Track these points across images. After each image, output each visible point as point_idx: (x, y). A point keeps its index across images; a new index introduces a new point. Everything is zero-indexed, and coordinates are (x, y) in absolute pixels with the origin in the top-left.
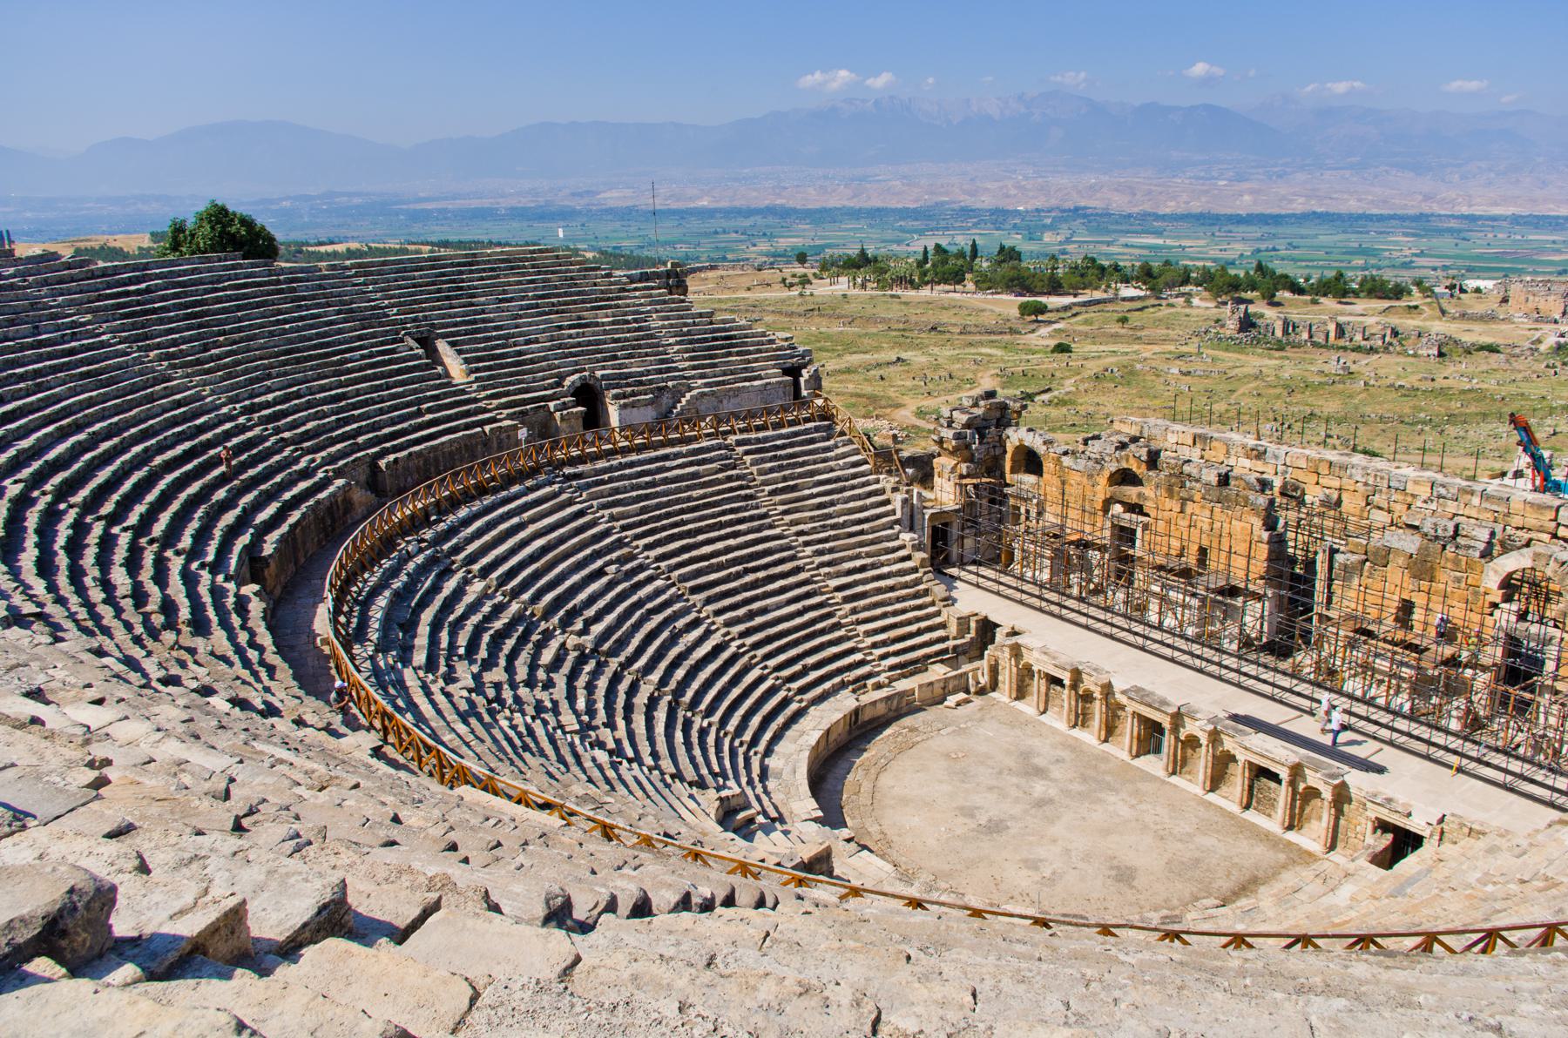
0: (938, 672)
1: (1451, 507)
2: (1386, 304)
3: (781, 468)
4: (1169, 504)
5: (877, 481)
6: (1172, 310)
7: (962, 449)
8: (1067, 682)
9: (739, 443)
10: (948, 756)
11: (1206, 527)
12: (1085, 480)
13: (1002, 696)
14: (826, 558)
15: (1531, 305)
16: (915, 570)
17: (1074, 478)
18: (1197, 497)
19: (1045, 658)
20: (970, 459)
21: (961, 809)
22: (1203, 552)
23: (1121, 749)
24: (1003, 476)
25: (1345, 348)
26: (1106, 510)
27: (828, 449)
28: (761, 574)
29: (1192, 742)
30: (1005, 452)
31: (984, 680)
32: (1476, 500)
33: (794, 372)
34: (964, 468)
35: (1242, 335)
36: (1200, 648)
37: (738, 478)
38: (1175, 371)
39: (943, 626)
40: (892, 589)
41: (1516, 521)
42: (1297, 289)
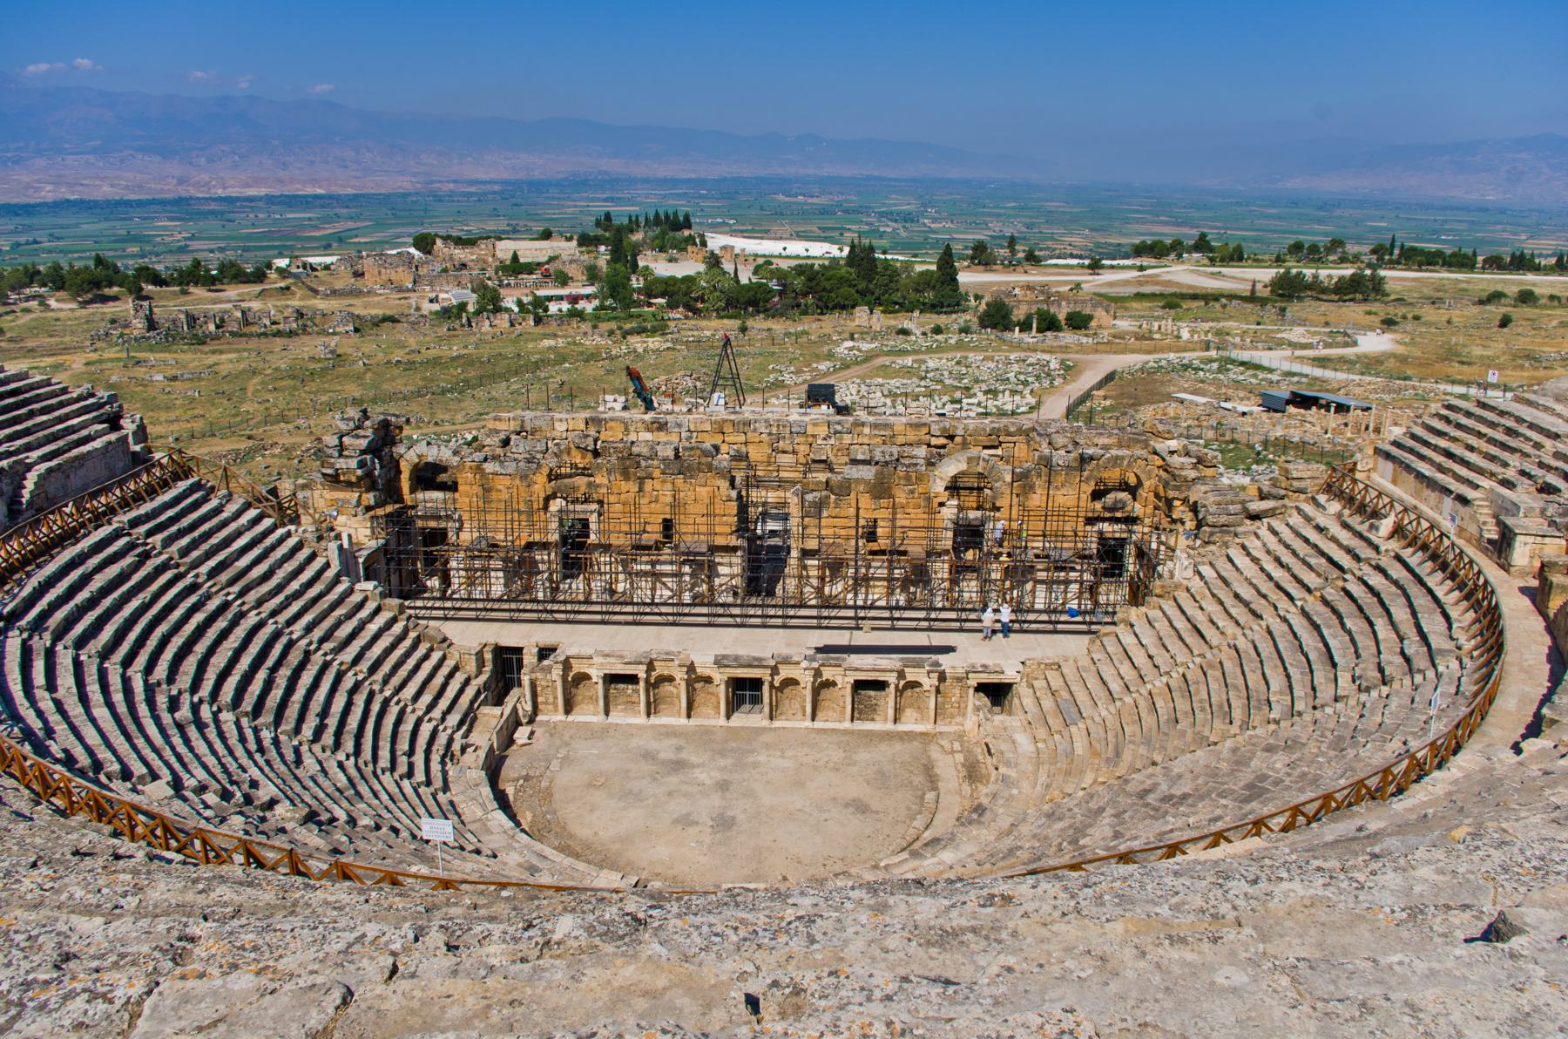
0: (492, 716)
1: (847, 439)
2: (258, 288)
3: (194, 545)
4: (624, 486)
5: (289, 534)
6: (33, 316)
7: (368, 481)
8: (642, 675)
9: (135, 523)
10: (590, 785)
11: (669, 499)
12: (517, 482)
13: (552, 715)
14: (318, 633)
15: (384, 277)
16: (394, 620)
17: (502, 484)
18: (657, 473)
19: (613, 660)
20: (372, 487)
21: (676, 821)
22: (668, 525)
23: (713, 717)
24: (401, 500)
25: (265, 334)
26: (546, 508)
27: (218, 511)
28: (284, 673)
29: (790, 682)
30: (399, 472)
31: (529, 708)
32: (867, 430)
33: (114, 422)
34: (369, 498)
35: (151, 334)
36: (706, 609)
37: (160, 570)
38: (159, 377)
39: (456, 669)
40: (393, 646)
41: (901, 440)
42: (158, 281)
